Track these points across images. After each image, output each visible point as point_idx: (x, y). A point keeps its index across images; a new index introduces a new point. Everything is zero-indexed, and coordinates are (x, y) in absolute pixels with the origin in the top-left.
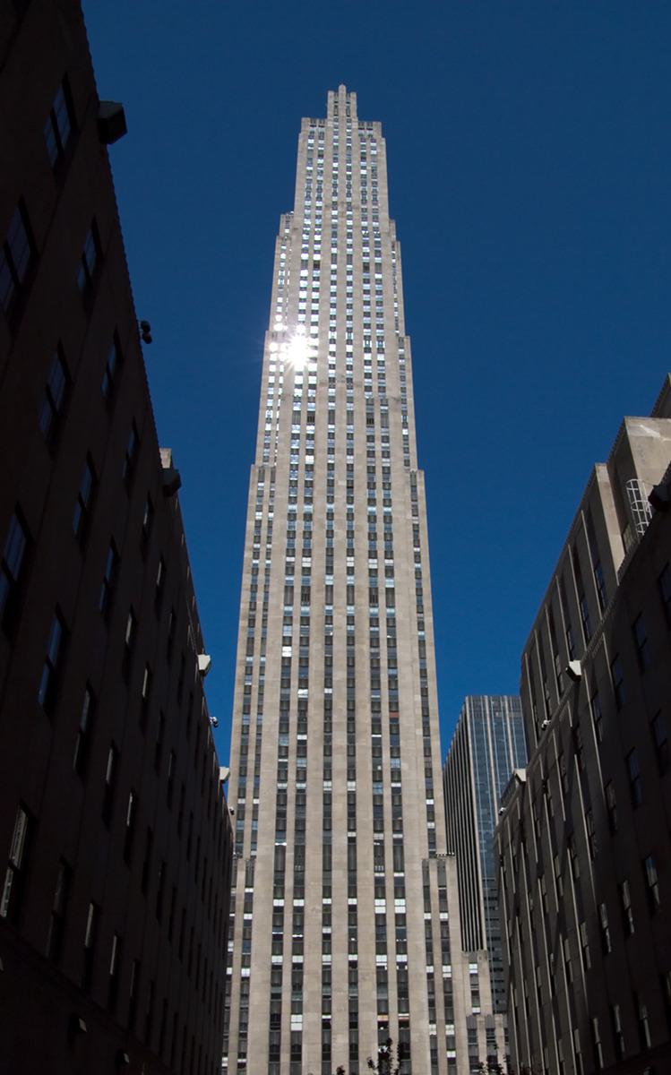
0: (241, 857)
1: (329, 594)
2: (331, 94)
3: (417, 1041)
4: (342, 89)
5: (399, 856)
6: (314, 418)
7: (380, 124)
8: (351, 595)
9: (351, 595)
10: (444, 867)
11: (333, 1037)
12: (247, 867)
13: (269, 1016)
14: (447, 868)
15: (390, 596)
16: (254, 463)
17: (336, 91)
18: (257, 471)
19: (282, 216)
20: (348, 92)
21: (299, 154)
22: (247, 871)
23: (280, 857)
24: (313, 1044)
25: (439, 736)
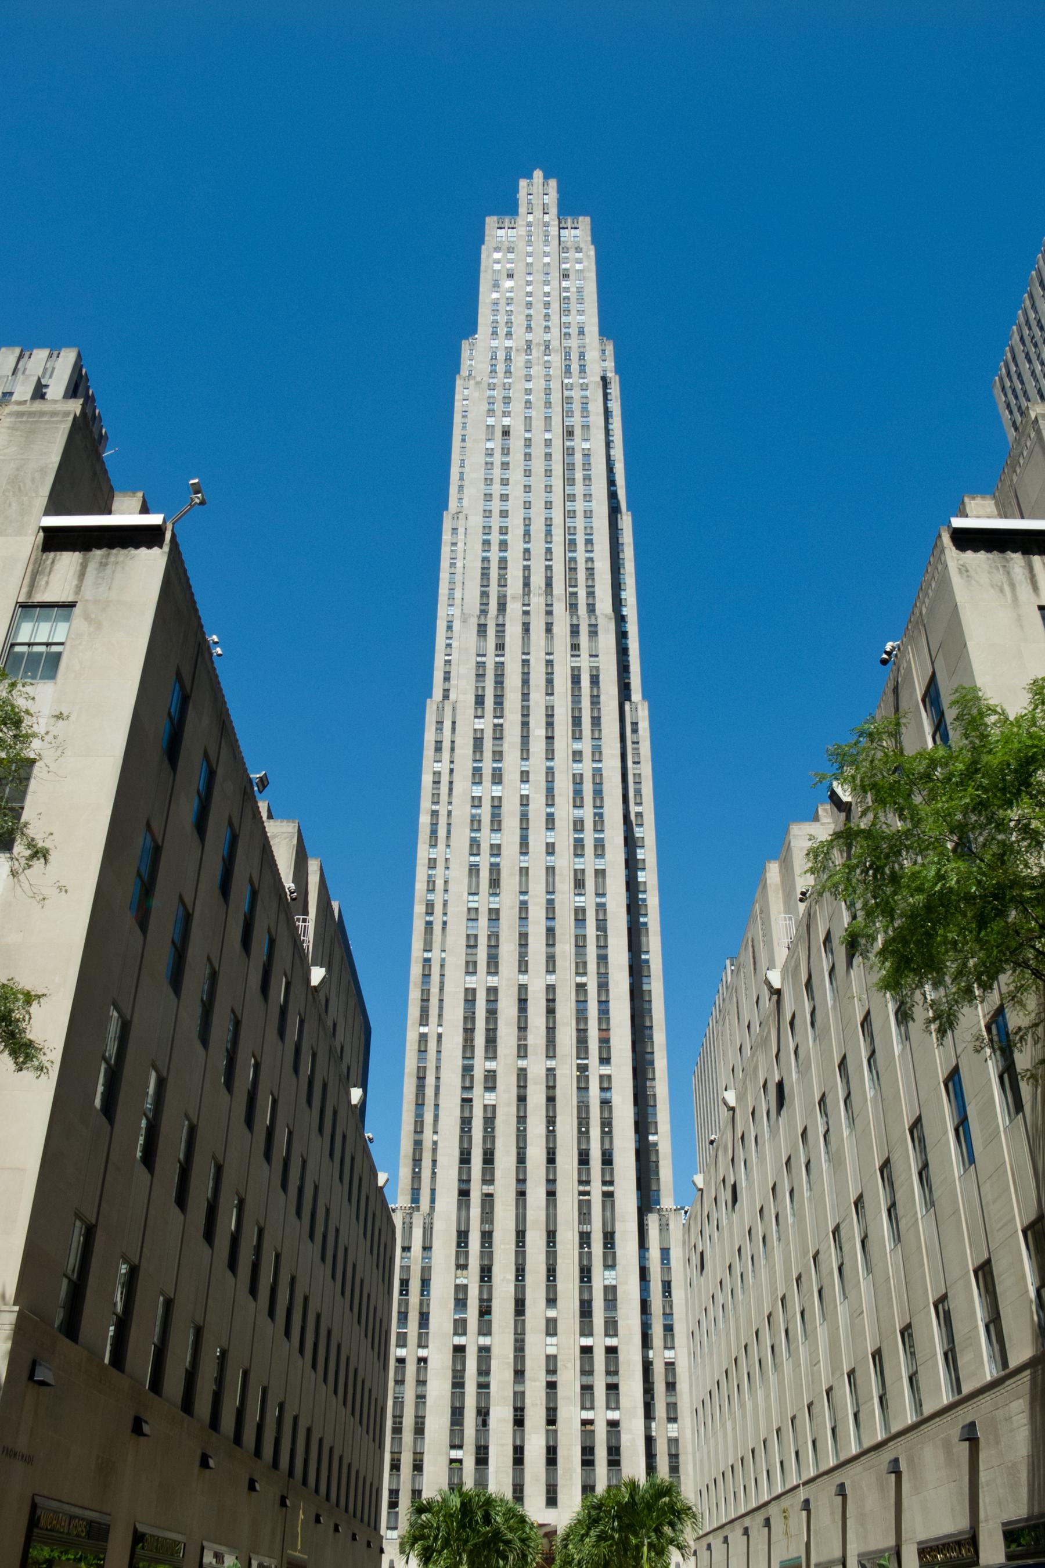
0: (418, 1210)
1: (524, 879)
2: (523, 183)
3: (629, 1444)
4: (538, 175)
5: (609, 1214)
6: (504, 644)
7: (588, 219)
8: (551, 879)
9: (551, 879)
10: (668, 1225)
11: (526, 1437)
12: (424, 1223)
13: (449, 1410)
14: (671, 1226)
15: (600, 880)
16: (431, 697)
17: (530, 176)
18: (435, 707)
19: (463, 342)
20: (546, 177)
21: (482, 275)
22: (424, 1228)
23: (464, 1213)
24: (502, 1445)
25: (665, 1053)
